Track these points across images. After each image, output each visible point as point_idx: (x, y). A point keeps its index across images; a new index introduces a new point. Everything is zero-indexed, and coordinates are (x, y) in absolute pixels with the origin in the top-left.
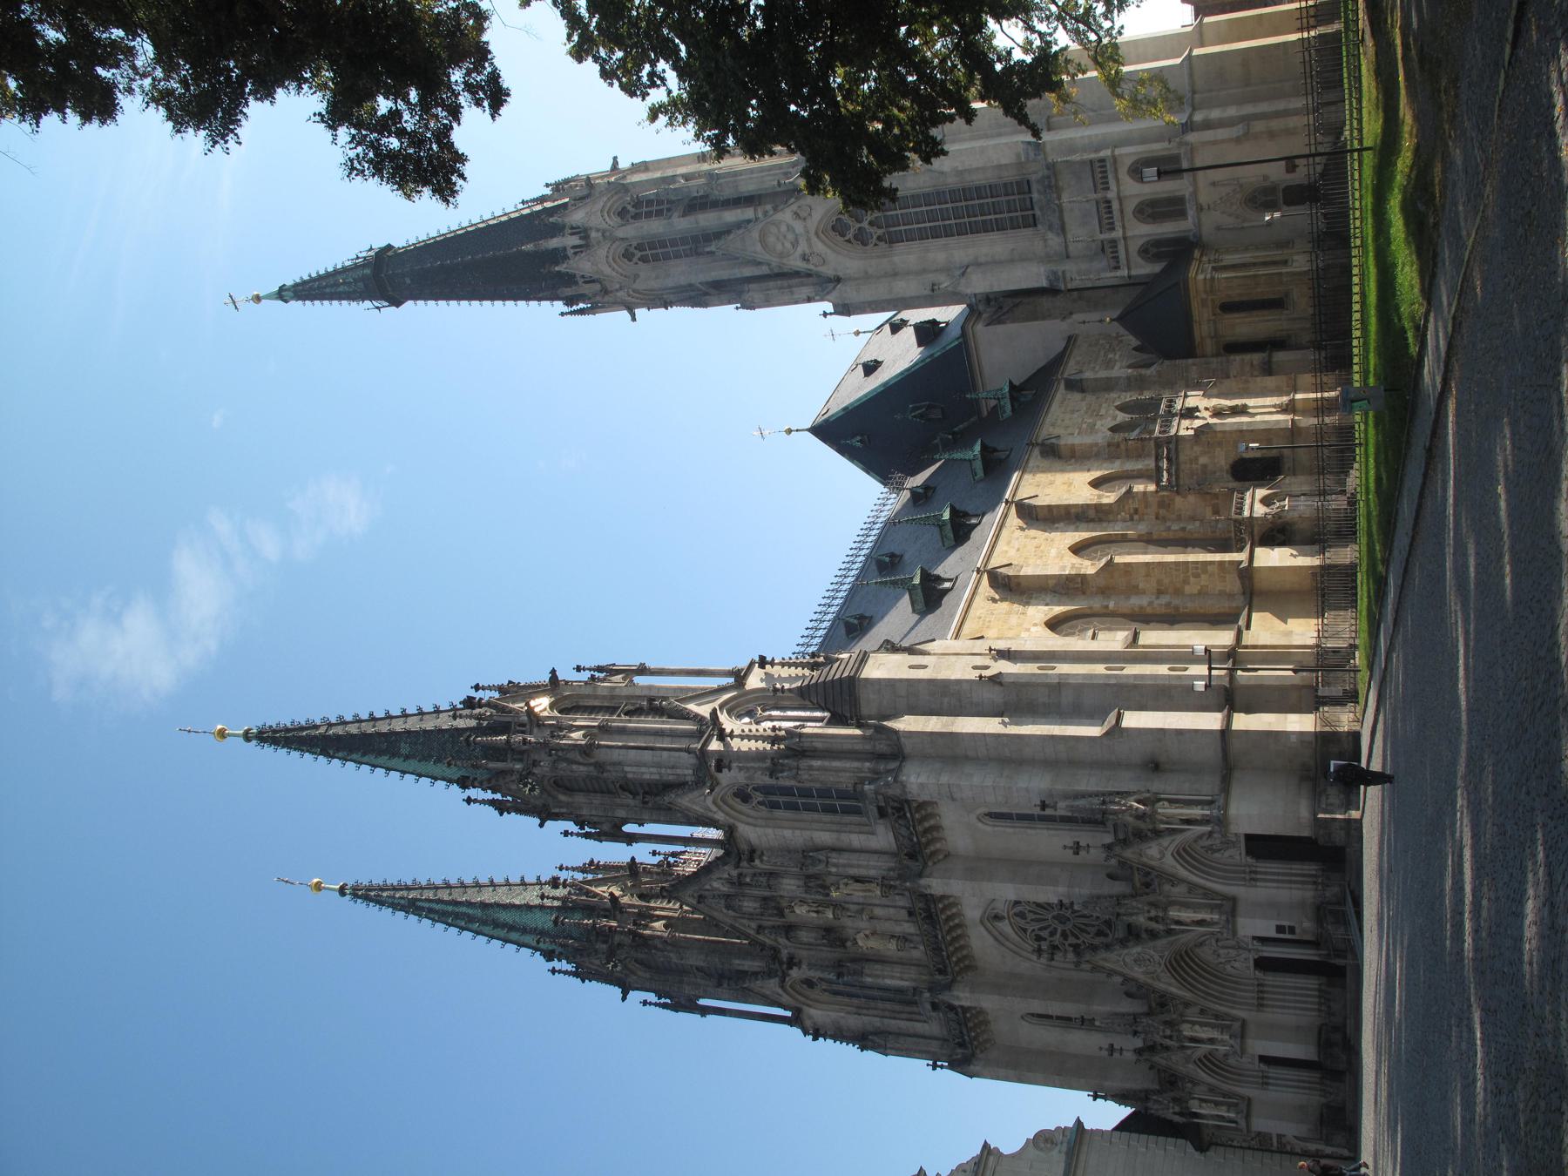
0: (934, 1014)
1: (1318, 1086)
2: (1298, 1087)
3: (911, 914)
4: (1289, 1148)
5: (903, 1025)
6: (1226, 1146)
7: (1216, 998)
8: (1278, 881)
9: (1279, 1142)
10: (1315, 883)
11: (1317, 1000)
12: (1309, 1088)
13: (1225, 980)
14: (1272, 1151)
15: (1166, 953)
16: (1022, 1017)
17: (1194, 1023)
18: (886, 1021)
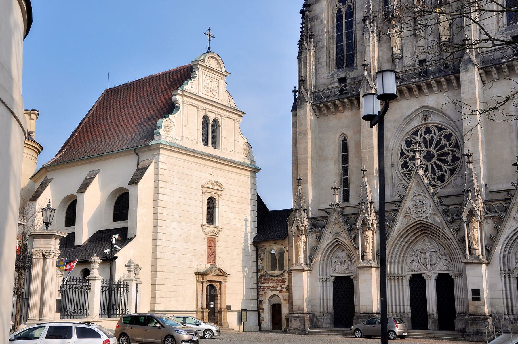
0: (336, 79)
1: (325, 311)
2: (323, 300)
3: (422, 62)
4: (261, 293)
5: (324, 59)
6: (257, 256)
7: (393, 250)
8: (506, 291)
9: (265, 288)
10: (508, 314)
11: (398, 312)
12: (324, 306)
13: (404, 257)
14: (257, 283)
15: (430, 221)
16: (343, 134)
17: (373, 238)
18: (325, 49)
